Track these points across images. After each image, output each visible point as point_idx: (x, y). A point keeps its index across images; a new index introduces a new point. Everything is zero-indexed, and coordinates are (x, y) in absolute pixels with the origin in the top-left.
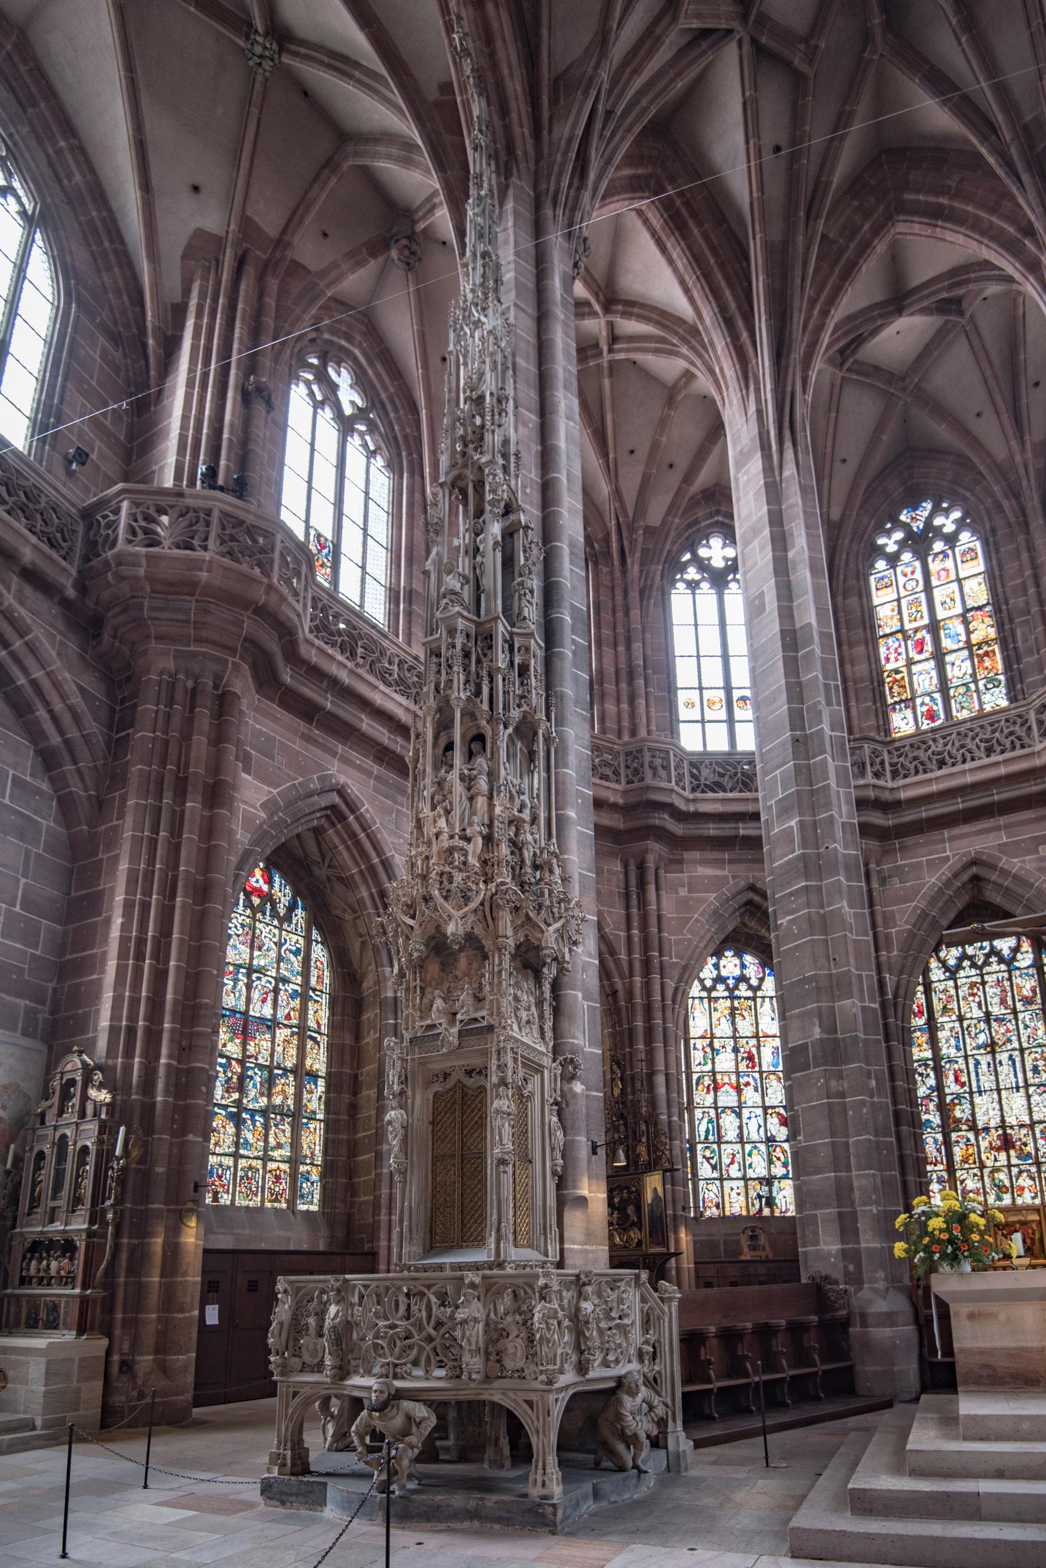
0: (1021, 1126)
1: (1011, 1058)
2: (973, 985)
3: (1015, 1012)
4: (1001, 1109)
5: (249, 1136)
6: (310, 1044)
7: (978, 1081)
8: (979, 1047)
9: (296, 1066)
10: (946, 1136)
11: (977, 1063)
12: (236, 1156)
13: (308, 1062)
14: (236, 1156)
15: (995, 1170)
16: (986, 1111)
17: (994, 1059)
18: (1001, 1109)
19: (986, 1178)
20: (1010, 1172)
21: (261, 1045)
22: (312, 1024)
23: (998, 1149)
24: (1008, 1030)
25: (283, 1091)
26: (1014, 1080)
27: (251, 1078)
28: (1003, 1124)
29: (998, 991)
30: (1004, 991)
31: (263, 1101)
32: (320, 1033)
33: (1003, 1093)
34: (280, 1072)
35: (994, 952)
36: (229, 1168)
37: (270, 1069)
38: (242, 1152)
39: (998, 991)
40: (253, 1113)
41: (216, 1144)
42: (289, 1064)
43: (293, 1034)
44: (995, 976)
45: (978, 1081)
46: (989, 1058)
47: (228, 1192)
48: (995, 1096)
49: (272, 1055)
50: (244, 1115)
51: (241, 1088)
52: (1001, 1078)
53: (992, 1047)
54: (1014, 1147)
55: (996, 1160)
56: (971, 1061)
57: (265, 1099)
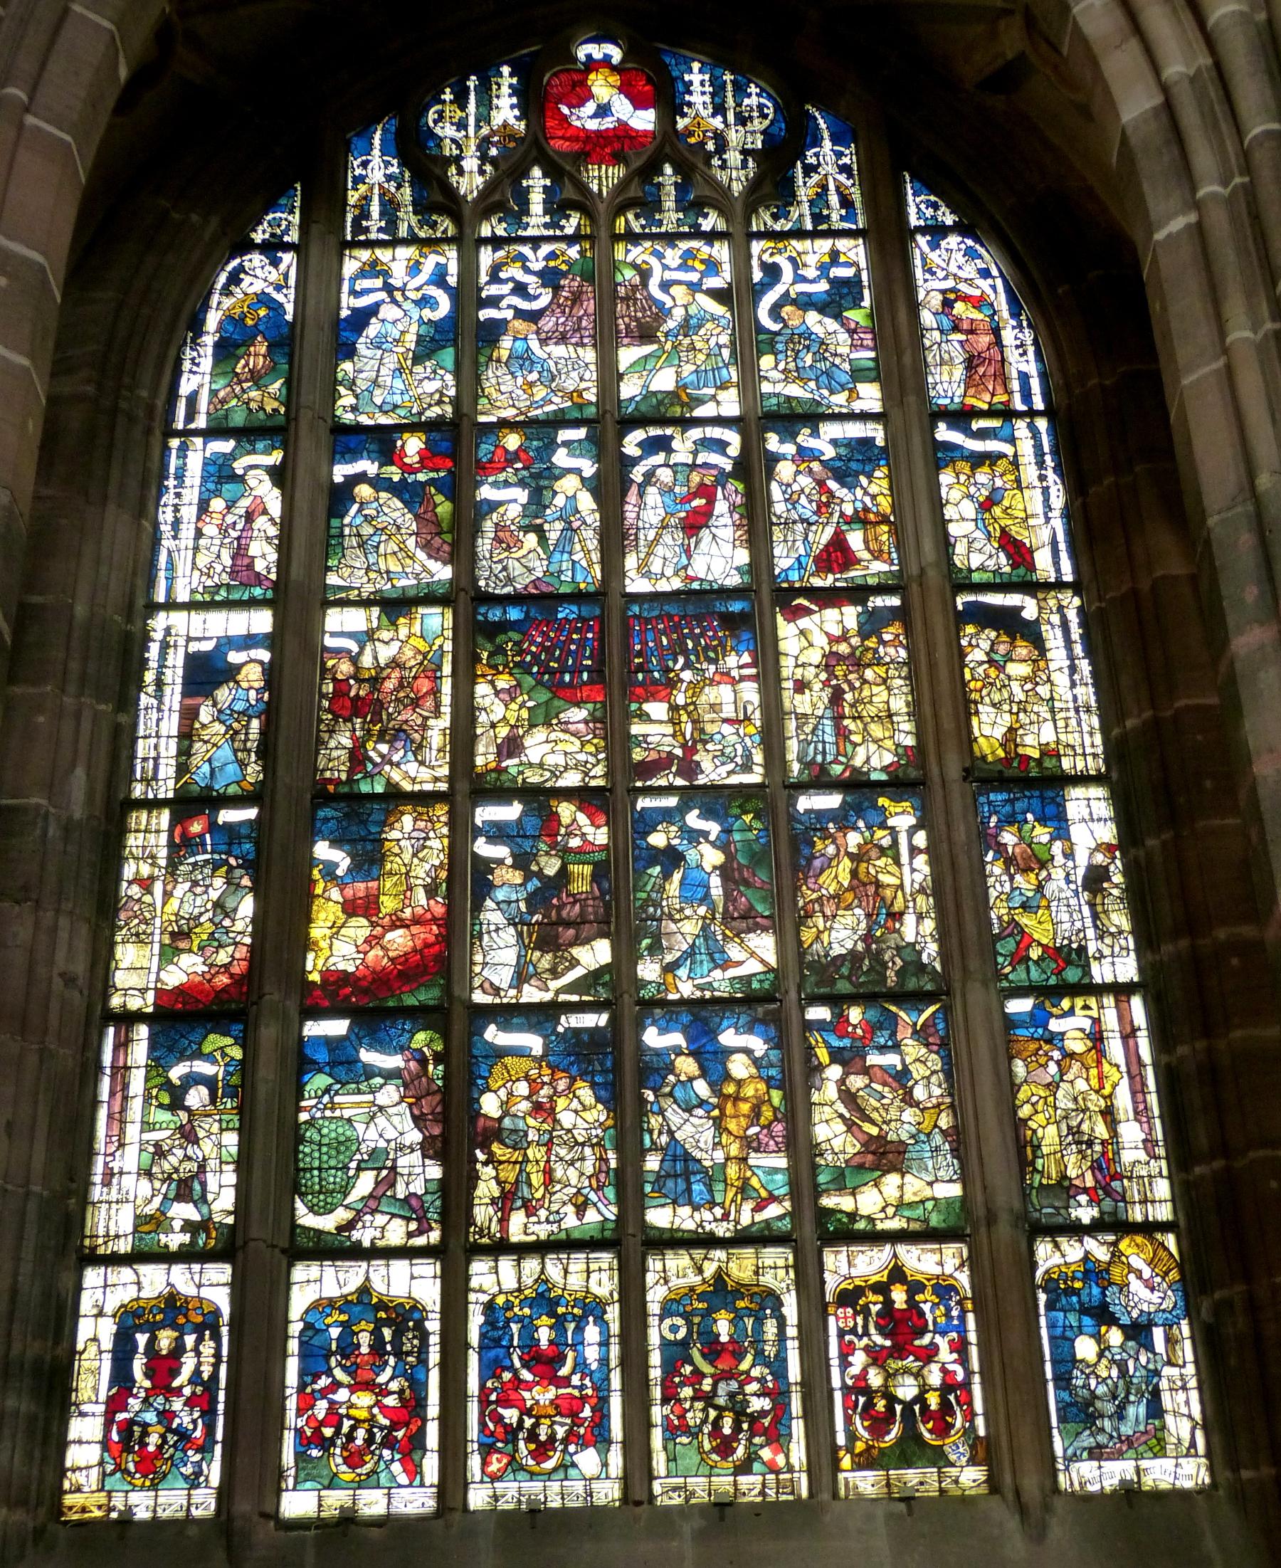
5: (695, 1132)
6: (978, 645)
9: (917, 755)
12: (631, 1244)
13: (989, 728)
14: (631, 1244)
21: (712, 715)
22: (975, 552)
25: (863, 887)
27: (672, 858)
31: (757, 953)
32: (1032, 587)
34: (833, 801)
36: (592, 1308)
37: (769, 800)
38: (659, 1217)
40: (702, 1015)
41: (506, 1201)
42: (875, 757)
43: (872, 624)
47: (599, 1438)
49: (772, 739)
50: (652, 1038)
51: (626, 920)
57: (765, 945)
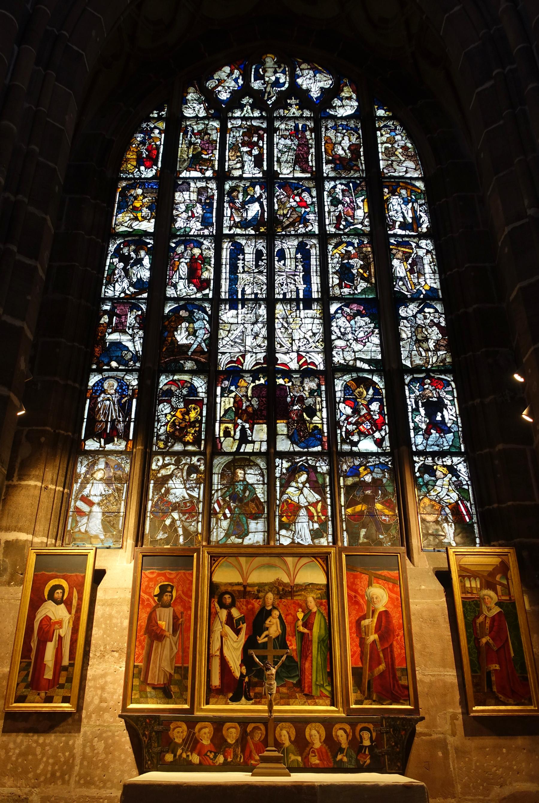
0: (307, 372)
1: (302, 248)
2: (251, 131)
3: (319, 179)
4: (271, 337)
7: (233, 280)
8: (244, 224)
10: (148, 379)
11: (238, 251)
15: (241, 460)
16: (240, 336)
17: (270, 247)
18: (271, 337)
19: (216, 478)
20: (271, 467)
23: (253, 418)
24: (302, 204)
26: (302, 287)
28: (270, 366)
29: (293, 143)
30: (304, 145)
33: (279, 307)
35: (295, 91)
39: (293, 143)
44: (292, 124)
45: (233, 280)
46: (261, 245)
48: (263, 311)
52: (278, 280)
53: (269, 228)
54: (285, 414)
55: (244, 439)
56: (226, 245)
